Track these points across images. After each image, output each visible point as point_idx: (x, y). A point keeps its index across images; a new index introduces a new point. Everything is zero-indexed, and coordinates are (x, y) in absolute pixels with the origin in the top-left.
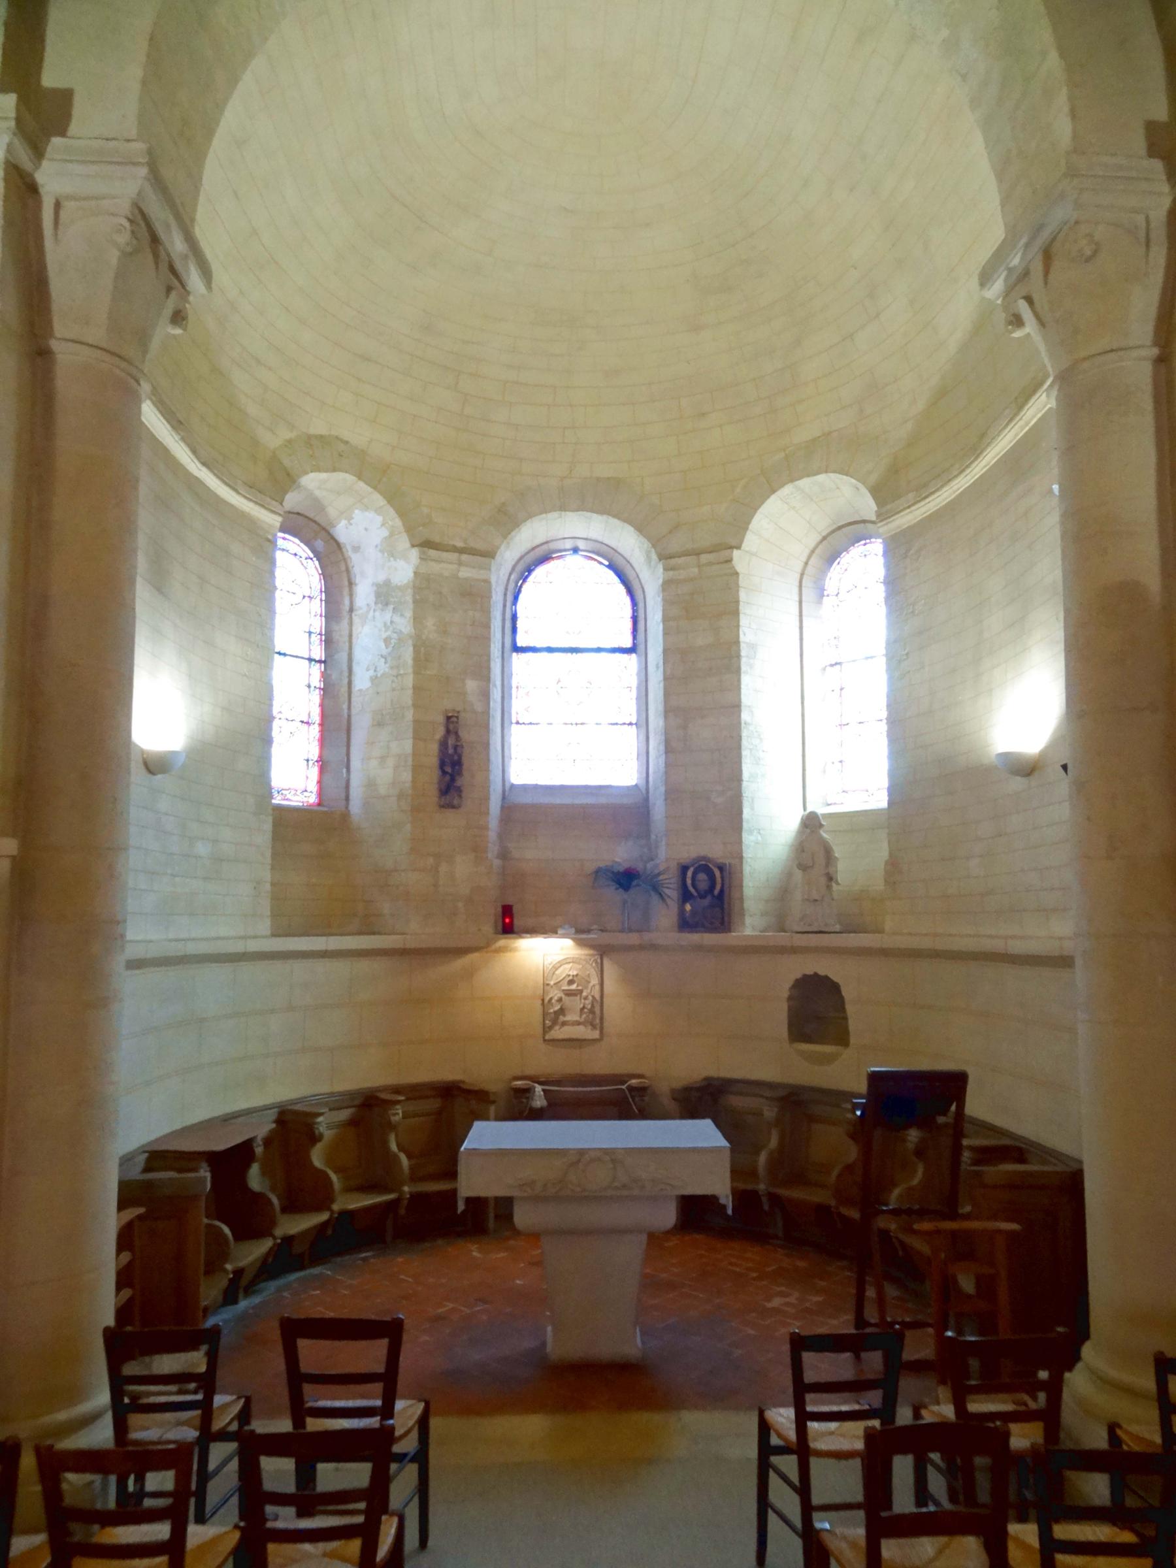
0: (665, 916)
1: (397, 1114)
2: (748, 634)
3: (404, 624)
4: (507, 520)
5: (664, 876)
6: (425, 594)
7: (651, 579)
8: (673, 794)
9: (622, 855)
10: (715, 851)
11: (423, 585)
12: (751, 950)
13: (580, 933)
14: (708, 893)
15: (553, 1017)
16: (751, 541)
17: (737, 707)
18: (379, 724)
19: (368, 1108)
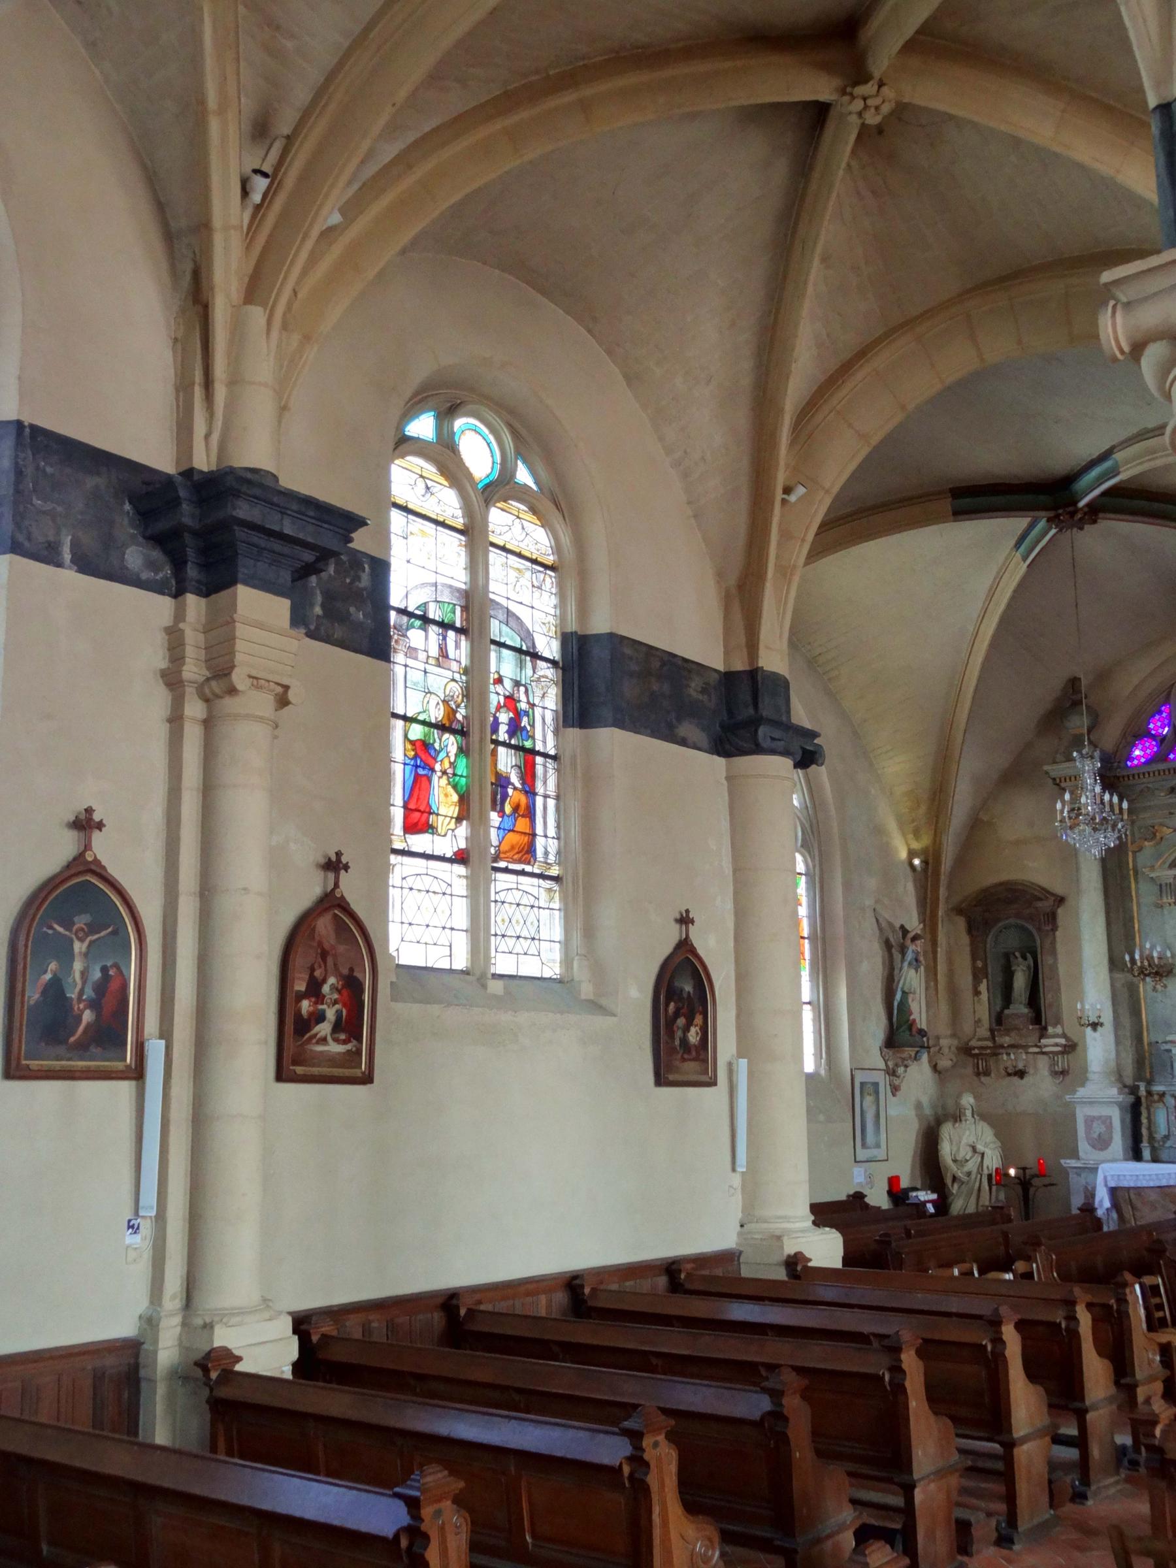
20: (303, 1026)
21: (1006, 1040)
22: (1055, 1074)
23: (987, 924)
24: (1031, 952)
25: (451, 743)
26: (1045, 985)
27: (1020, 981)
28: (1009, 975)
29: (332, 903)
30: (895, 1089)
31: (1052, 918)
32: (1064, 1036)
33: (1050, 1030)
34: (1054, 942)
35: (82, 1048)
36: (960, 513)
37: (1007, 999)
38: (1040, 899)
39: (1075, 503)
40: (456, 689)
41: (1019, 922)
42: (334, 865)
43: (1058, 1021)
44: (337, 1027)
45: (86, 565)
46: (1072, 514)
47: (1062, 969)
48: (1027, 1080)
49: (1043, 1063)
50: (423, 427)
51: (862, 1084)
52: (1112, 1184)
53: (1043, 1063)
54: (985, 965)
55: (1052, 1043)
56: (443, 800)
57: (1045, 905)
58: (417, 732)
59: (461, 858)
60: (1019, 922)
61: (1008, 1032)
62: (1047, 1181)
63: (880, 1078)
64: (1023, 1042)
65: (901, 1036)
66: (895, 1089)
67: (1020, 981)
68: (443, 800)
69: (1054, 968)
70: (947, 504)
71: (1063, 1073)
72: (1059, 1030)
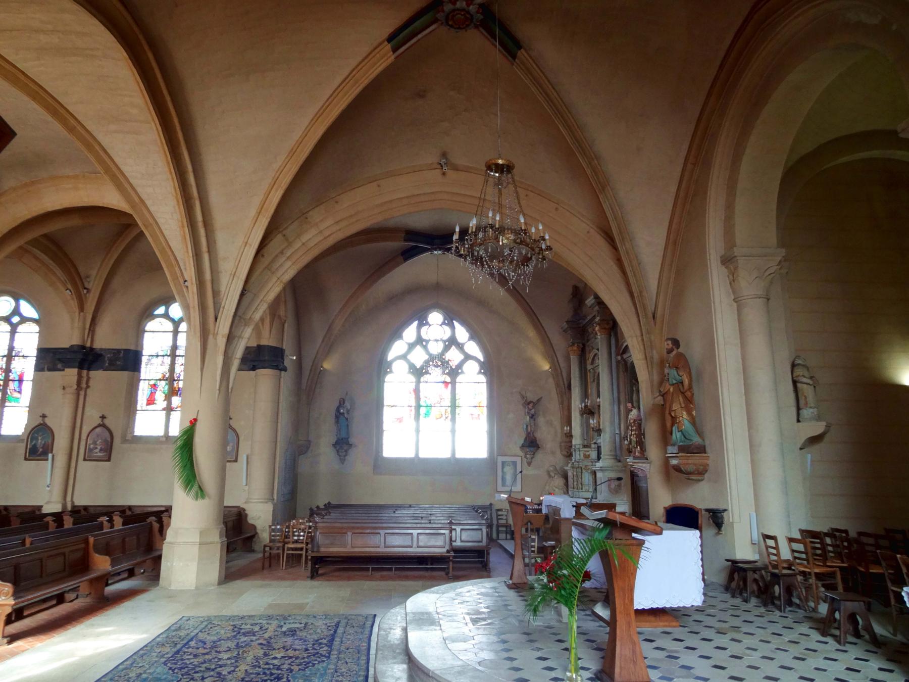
20: (91, 450)
25: (163, 383)
29: (103, 425)
30: (529, 464)
35: (40, 455)
36: (406, 259)
40: (167, 370)
42: (103, 417)
44: (101, 450)
45: (49, 370)
50: (161, 310)
51: (503, 463)
56: (160, 396)
58: (152, 382)
59: (164, 409)
63: (518, 460)
65: (532, 444)
66: (529, 464)
68: (160, 396)
70: (401, 258)
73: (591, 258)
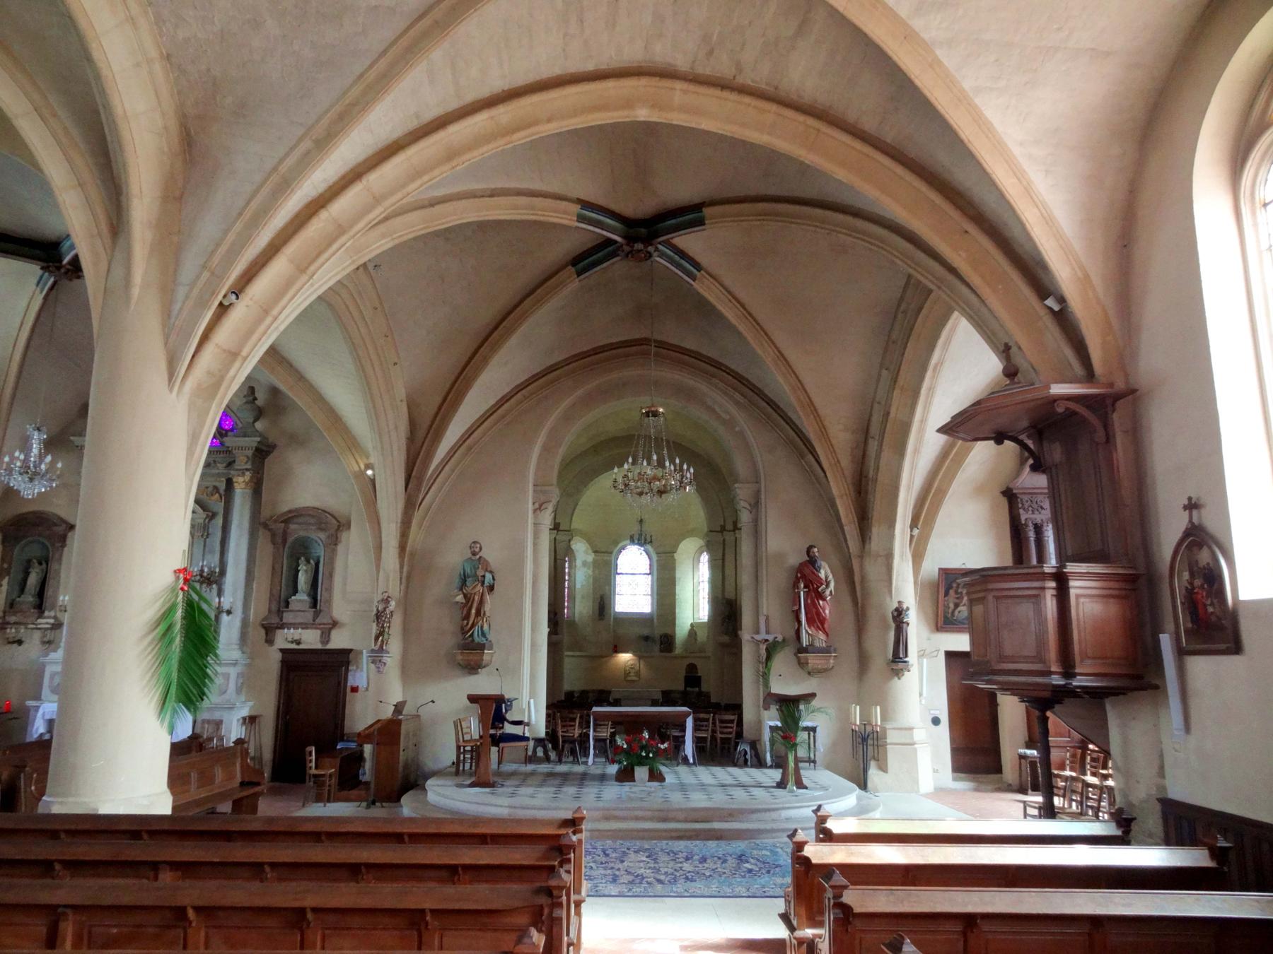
0: (657, 648)
1: (591, 695)
2: (678, 575)
3: (590, 572)
4: (616, 543)
5: (655, 635)
6: (596, 564)
7: (655, 557)
8: (659, 616)
9: (646, 632)
10: (669, 632)
11: (595, 562)
12: (676, 657)
13: (634, 653)
14: (667, 642)
15: (627, 674)
16: (679, 551)
17: (674, 594)
18: (583, 597)
19: (584, 693)
21: (13, 619)
22: (44, 643)
23: (17, 539)
24: (45, 561)
26: (51, 583)
27: (33, 579)
28: (27, 574)
31: (63, 539)
32: (55, 617)
33: (47, 613)
34: (61, 555)
37: (22, 590)
38: (56, 525)
39: (61, 261)
41: (41, 539)
43: (53, 607)
46: (59, 268)
47: (63, 575)
48: (24, 646)
49: (37, 635)
52: (48, 717)
53: (37, 635)
54: (10, 567)
55: (45, 622)
57: (60, 529)
60: (41, 539)
61: (15, 614)
62: (10, 716)
64: (24, 621)
67: (33, 579)
69: (58, 573)
71: (49, 642)
72: (52, 614)
73: (396, 428)
